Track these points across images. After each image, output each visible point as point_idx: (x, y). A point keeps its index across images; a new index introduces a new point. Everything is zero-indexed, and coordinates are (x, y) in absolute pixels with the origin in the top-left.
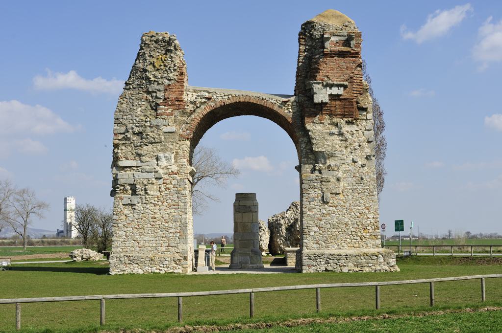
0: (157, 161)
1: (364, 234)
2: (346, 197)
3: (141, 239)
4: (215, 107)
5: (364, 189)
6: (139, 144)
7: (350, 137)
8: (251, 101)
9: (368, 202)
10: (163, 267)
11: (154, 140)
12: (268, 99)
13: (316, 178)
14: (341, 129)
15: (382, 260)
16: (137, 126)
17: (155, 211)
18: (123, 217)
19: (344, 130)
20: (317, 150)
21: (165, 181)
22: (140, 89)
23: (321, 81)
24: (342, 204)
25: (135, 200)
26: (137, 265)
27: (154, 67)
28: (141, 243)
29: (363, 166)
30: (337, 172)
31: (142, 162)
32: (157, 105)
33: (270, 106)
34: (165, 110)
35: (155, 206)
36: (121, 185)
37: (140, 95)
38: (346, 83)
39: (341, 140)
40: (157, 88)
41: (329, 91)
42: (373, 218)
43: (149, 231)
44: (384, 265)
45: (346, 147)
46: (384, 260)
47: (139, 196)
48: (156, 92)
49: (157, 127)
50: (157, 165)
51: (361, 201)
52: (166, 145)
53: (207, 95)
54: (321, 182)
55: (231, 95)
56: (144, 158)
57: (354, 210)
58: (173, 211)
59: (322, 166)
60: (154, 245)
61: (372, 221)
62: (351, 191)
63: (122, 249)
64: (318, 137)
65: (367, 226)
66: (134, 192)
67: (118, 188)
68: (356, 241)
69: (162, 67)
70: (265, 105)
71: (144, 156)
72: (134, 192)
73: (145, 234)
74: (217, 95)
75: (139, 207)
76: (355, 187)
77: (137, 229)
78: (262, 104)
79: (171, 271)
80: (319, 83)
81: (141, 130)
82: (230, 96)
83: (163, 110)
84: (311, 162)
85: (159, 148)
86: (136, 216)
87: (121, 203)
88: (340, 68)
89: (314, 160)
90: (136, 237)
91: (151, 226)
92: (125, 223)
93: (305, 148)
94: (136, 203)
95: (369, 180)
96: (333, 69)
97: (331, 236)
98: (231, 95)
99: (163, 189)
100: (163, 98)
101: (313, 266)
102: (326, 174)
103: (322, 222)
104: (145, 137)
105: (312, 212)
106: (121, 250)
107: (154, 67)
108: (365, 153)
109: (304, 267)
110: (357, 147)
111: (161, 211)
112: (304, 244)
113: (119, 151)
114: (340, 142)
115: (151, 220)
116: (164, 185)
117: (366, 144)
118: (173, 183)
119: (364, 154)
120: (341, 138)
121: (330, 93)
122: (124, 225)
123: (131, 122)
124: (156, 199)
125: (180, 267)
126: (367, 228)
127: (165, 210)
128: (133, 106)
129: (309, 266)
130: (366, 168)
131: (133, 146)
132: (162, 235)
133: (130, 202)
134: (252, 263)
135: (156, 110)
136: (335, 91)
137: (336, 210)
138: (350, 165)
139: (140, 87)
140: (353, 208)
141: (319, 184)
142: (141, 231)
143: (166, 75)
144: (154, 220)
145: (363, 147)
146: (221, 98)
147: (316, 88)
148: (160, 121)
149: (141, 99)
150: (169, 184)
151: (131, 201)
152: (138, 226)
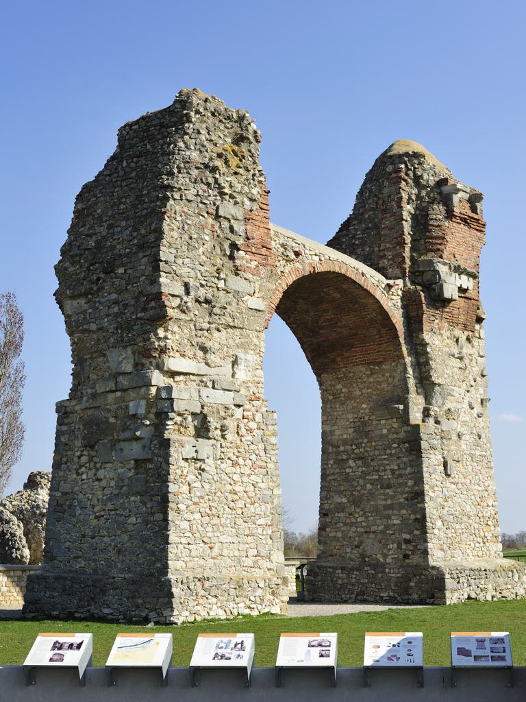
1: (486, 534)
2: (466, 467)
3: (215, 540)
6: (206, 326)
8: (348, 275)
10: (255, 603)
11: (234, 321)
13: (436, 431)
14: (461, 349)
15: (516, 579)
16: (202, 286)
17: (236, 477)
18: (185, 488)
22: (201, 205)
24: (463, 480)
25: (205, 448)
26: (214, 600)
28: (216, 551)
31: (207, 364)
32: (234, 246)
33: (372, 291)
36: (180, 414)
37: (201, 217)
39: (460, 368)
40: (233, 213)
43: (228, 521)
47: (212, 441)
48: (229, 221)
57: (475, 491)
60: (237, 553)
61: (493, 512)
63: (186, 563)
66: (202, 431)
67: (172, 419)
69: (241, 171)
72: (202, 431)
73: (221, 529)
75: (210, 465)
76: (473, 452)
78: (362, 284)
80: (445, 264)
81: (209, 296)
83: (244, 262)
85: (238, 341)
86: (207, 486)
92: (189, 502)
94: (204, 457)
99: (243, 431)
102: (445, 425)
104: (219, 312)
106: (184, 565)
109: (448, 594)
113: (169, 335)
115: (230, 497)
116: (246, 421)
117: (478, 379)
118: (256, 419)
119: (478, 396)
121: (459, 286)
123: (192, 274)
124: (236, 451)
125: (277, 601)
127: (249, 475)
128: (191, 238)
131: (193, 327)
133: (195, 455)
135: (232, 257)
139: (202, 202)
140: (473, 487)
142: (216, 521)
144: (235, 497)
147: (443, 269)
151: (196, 451)
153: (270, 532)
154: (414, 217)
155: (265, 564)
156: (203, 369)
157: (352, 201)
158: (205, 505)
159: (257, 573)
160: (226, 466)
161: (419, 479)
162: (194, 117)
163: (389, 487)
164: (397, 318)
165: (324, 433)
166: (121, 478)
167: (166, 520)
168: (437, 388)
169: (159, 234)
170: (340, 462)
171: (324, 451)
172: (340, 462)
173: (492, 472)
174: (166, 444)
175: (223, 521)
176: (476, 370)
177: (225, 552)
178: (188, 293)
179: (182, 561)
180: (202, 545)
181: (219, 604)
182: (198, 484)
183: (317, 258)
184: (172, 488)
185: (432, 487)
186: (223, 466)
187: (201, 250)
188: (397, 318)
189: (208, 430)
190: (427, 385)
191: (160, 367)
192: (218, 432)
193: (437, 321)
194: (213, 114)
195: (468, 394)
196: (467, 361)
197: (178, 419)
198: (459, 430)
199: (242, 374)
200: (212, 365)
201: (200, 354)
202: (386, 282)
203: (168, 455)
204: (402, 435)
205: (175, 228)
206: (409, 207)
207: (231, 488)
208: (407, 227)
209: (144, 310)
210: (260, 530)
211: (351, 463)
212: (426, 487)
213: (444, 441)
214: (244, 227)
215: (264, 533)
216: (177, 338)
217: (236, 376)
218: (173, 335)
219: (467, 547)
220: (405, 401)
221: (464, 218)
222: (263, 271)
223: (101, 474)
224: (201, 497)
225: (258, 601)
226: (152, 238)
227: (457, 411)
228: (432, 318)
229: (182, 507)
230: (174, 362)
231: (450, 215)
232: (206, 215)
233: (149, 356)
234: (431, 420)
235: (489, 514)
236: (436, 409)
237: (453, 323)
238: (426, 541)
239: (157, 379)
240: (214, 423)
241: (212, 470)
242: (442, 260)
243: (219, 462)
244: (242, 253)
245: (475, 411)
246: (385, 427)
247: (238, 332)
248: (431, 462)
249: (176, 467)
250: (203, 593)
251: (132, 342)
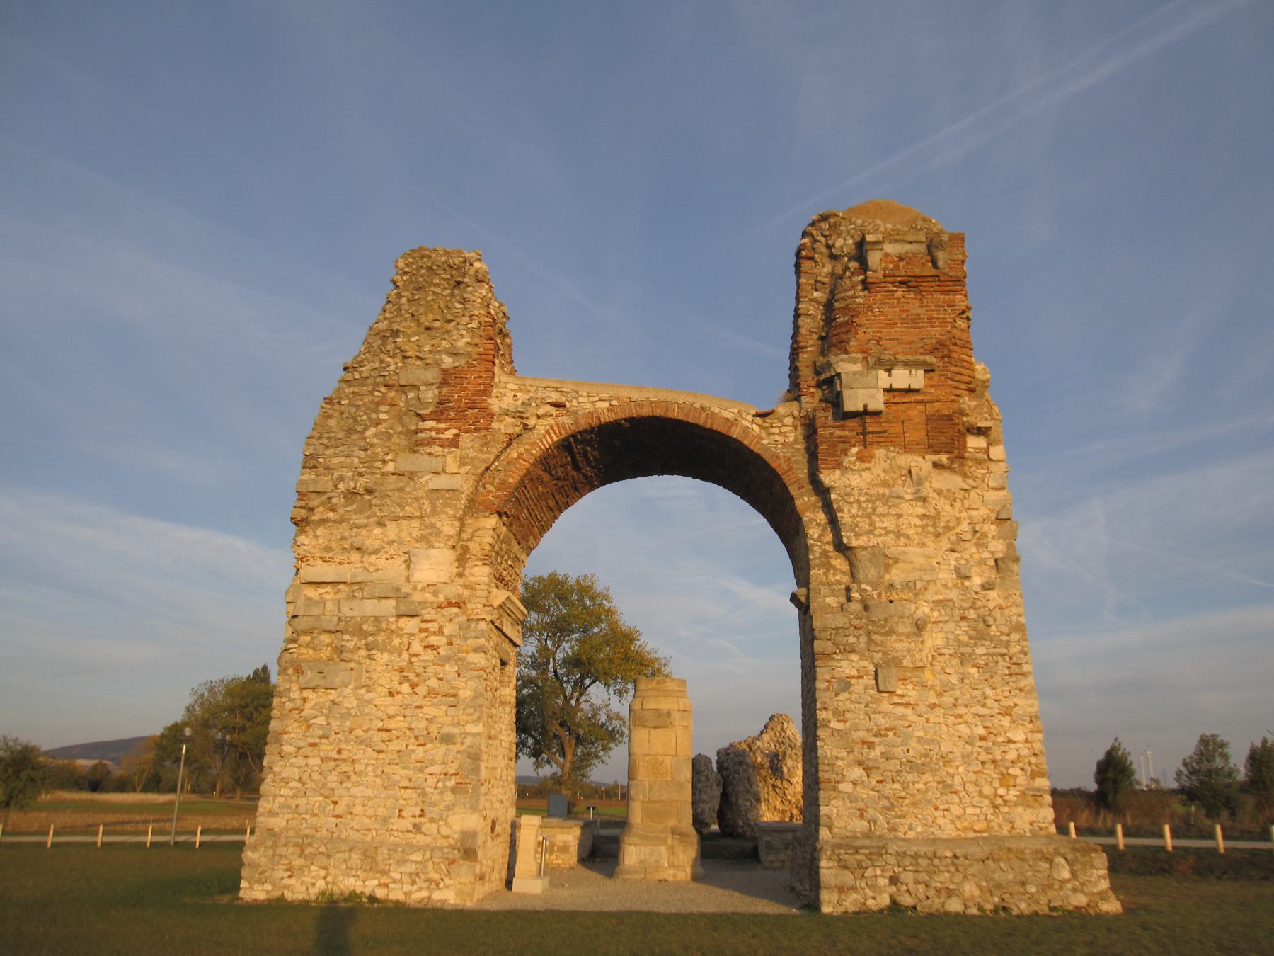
0: (408, 567)
1: (1001, 791)
4: (573, 428)
5: (992, 655)
7: (948, 507)
8: (670, 415)
9: (1007, 694)
10: (401, 881)
12: (717, 410)
15: (1066, 874)
17: (391, 711)
19: (927, 490)
20: (854, 543)
21: (424, 626)
23: (860, 356)
26: (323, 873)
27: (419, 323)
28: (340, 809)
29: (987, 586)
30: (913, 607)
34: (438, 431)
35: (391, 694)
38: (931, 359)
39: (924, 516)
40: (422, 377)
41: (883, 379)
42: (1026, 741)
43: (370, 769)
44: (1074, 890)
45: (938, 535)
46: (1074, 874)
49: (412, 476)
50: (408, 579)
51: (989, 692)
52: (433, 526)
53: (554, 397)
54: (869, 634)
55: (618, 399)
56: (374, 557)
57: (969, 718)
58: (442, 713)
59: (869, 588)
60: (381, 811)
61: (1025, 752)
62: (955, 661)
64: (855, 506)
65: (1009, 764)
68: (978, 811)
70: (708, 426)
71: (376, 552)
73: (354, 778)
74: (581, 399)
77: (335, 760)
78: (701, 423)
79: (424, 894)
80: (855, 361)
81: (370, 485)
82: (615, 403)
84: (838, 577)
87: (295, 687)
88: (914, 322)
89: (844, 573)
90: (329, 785)
91: (375, 755)
92: (302, 744)
93: (819, 540)
94: (338, 681)
95: (1006, 630)
96: (892, 324)
97: (903, 794)
98: (618, 399)
99: (417, 647)
100: (437, 400)
101: (853, 888)
103: (875, 753)
105: (845, 721)
106: (283, 823)
107: (419, 323)
108: (992, 553)
109: (824, 895)
110: (968, 536)
111: (407, 712)
112: (823, 820)
114: (918, 522)
117: (991, 529)
118: (447, 631)
119: (986, 555)
120: (920, 510)
121: (888, 386)
122: (299, 748)
125: (448, 881)
126: (1011, 771)
127: (421, 707)
129: (841, 889)
130: (992, 594)
132: (405, 783)
133: (321, 683)
134: (672, 866)
136: (901, 378)
137: (913, 718)
138: (950, 585)
141: (863, 639)
143: (445, 344)
144: (385, 735)
145: (984, 535)
146: (589, 406)
147: (847, 367)
148: (419, 461)
149: (378, 404)
150: (434, 633)
152: (339, 752)
153: (451, 783)
158: (330, 748)
159: (420, 839)
168: (862, 554)
173: (1023, 683)
175: (359, 767)
177: (358, 809)
180: (321, 799)
181: (329, 879)
182: (321, 720)
183: (605, 405)
186: (368, 696)
187: (371, 431)
190: (841, 547)
192: (363, 653)
193: (854, 450)
194: (430, 268)
195: (957, 555)
198: (919, 614)
200: (371, 569)
201: (355, 556)
205: (337, 414)
206: (816, 294)
207: (380, 725)
210: (431, 781)
213: (875, 637)
214: (436, 392)
215: (440, 785)
216: (321, 541)
217: (413, 579)
219: (939, 813)
221: (901, 283)
222: (466, 439)
224: (320, 737)
225: (406, 879)
228: (841, 446)
229: (288, 749)
232: (383, 389)
234: (855, 607)
235: (1012, 755)
236: (864, 586)
242: (845, 356)
243: (363, 691)
245: (977, 580)
247: (416, 523)
249: (284, 699)
250: (302, 861)
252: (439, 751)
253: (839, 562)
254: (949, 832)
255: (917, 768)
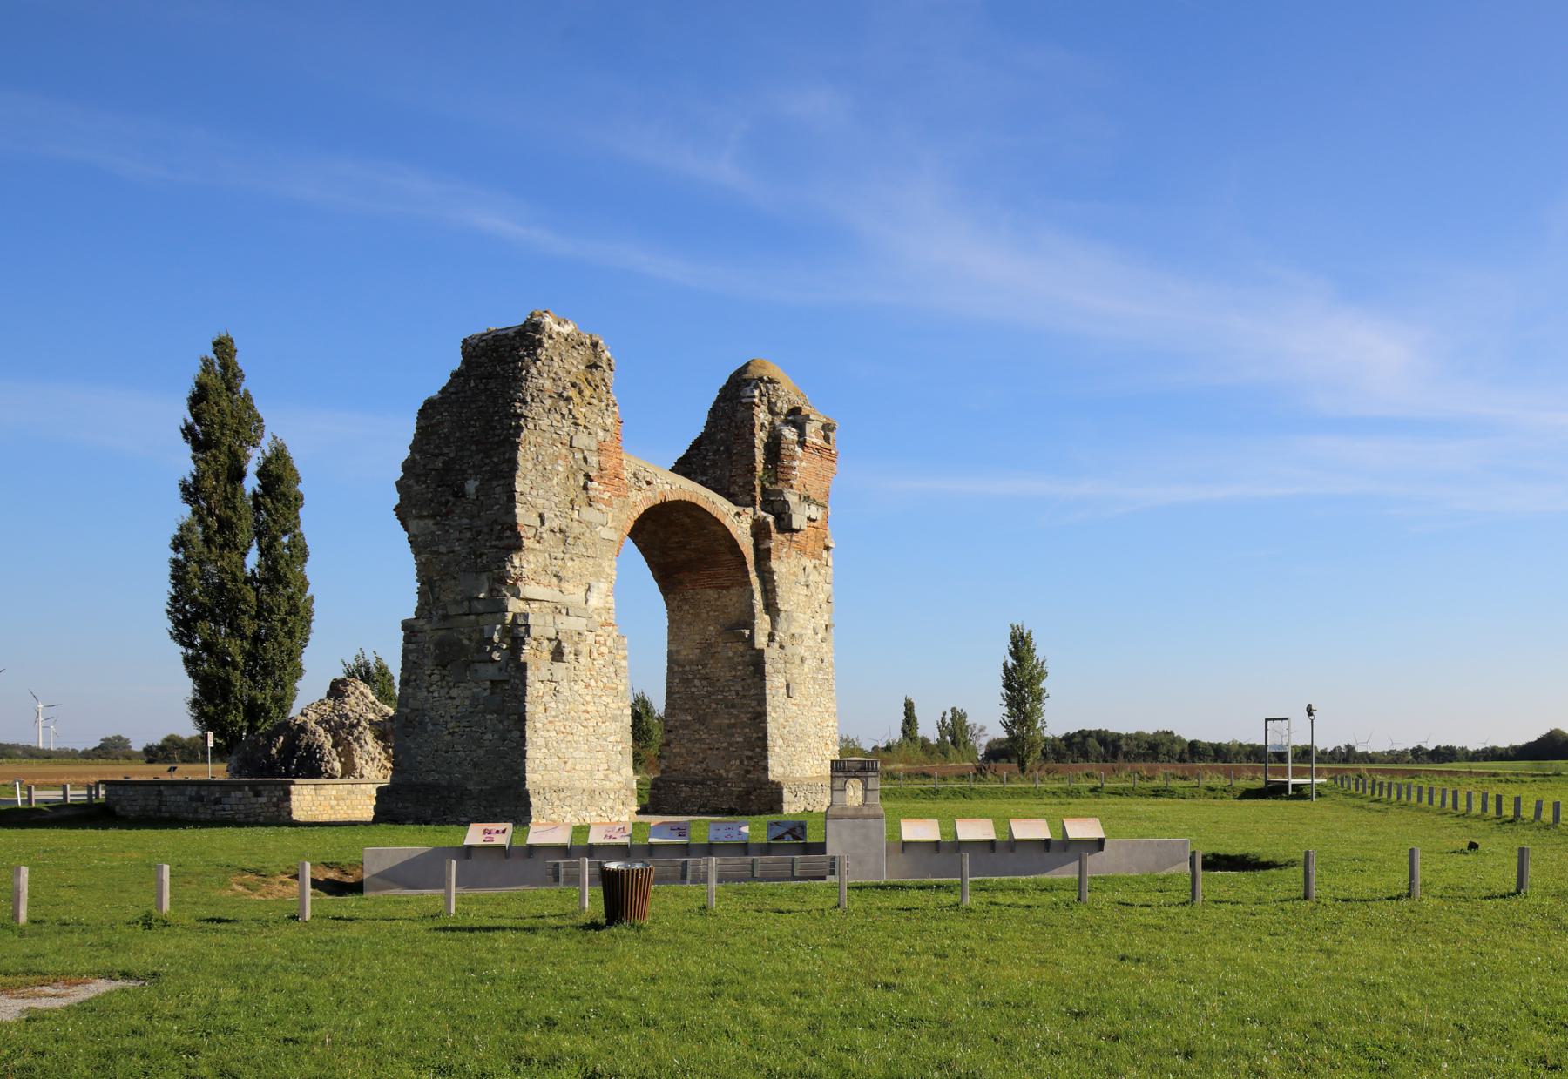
17: (588, 698)
18: (541, 709)
32: (588, 477)
49: (590, 525)
66: (557, 655)
72: (557, 655)
75: (564, 687)
86: (561, 706)
99: (595, 655)
102: (789, 650)
135: (585, 488)
147: (792, 498)
154: (767, 446)
155: (616, 777)
156: (558, 597)
157: (704, 418)
160: (579, 687)
161: (762, 700)
162: (547, 343)
163: (733, 706)
164: (746, 544)
165: (671, 655)
166: (475, 699)
167: (523, 737)
169: (513, 465)
170: (686, 682)
171: (670, 669)
172: (686, 682)
174: (523, 667)
176: (823, 597)
178: (543, 523)
179: (534, 776)
182: (553, 705)
184: (529, 708)
185: (774, 708)
188: (746, 544)
189: (562, 654)
190: (771, 608)
191: (516, 595)
196: (812, 588)
197: (534, 644)
199: (594, 601)
201: (555, 580)
202: (736, 509)
203: (525, 677)
204: (747, 658)
208: (760, 456)
209: (499, 538)
211: (697, 682)
212: (769, 709)
218: (525, 563)
220: (751, 627)
222: (615, 501)
223: (454, 693)
226: (505, 467)
227: (801, 635)
230: (528, 590)
231: (802, 444)
233: (502, 582)
234: (776, 645)
237: (802, 551)
238: (766, 758)
239: (514, 606)
240: (568, 649)
241: (567, 693)
244: (595, 484)
246: (732, 650)
247: (591, 562)
248: (774, 684)
251: (486, 568)
252: (612, 726)
253: (767, 617)
254: (809, 774)
255: (799, 739)
